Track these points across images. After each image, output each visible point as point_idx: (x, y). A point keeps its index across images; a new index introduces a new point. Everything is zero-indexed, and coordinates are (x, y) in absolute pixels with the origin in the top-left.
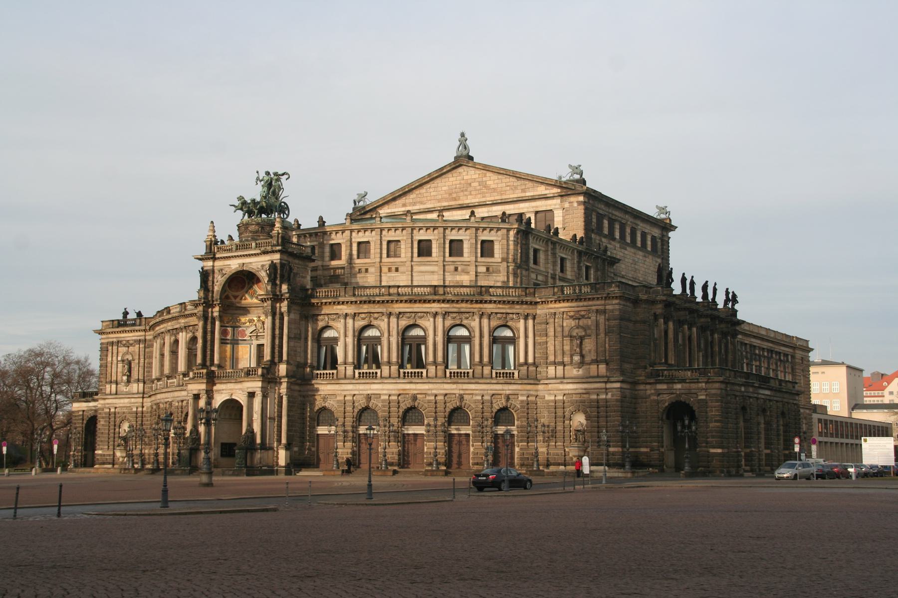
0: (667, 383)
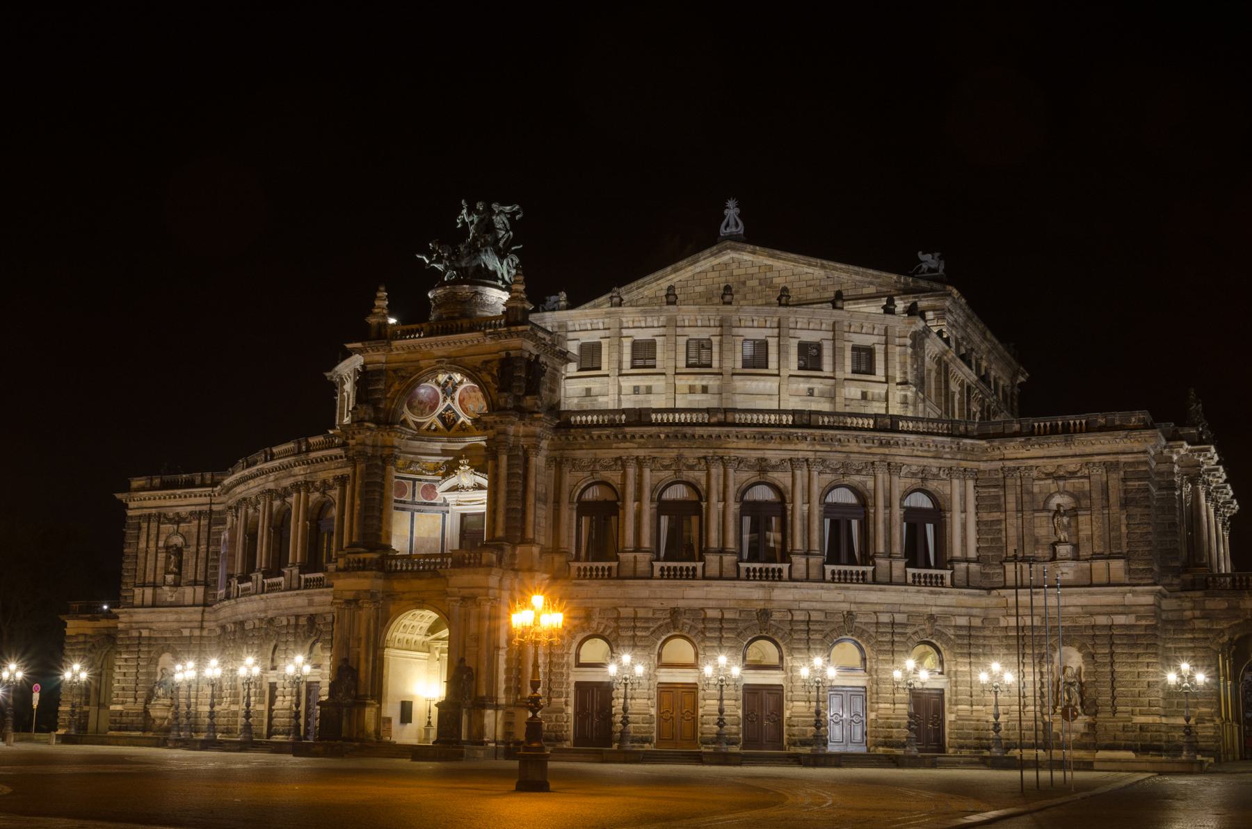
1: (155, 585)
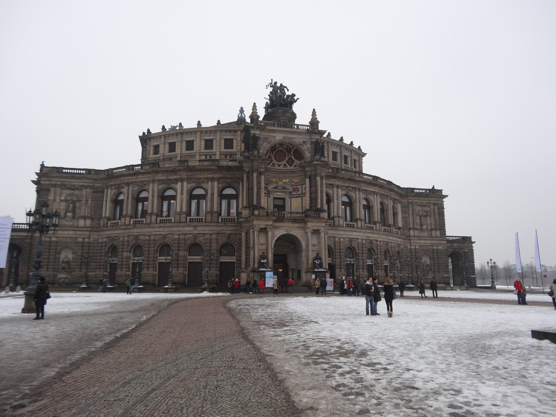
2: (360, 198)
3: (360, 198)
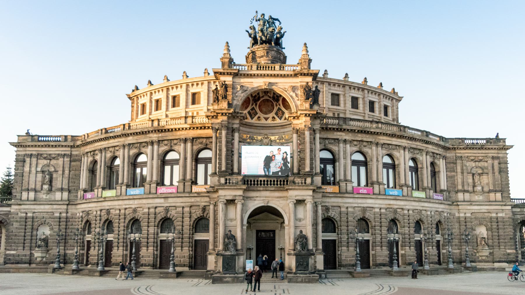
0: (520, 208)
1: (35, 191)
2: (377, 155)
3: (377, 155)
